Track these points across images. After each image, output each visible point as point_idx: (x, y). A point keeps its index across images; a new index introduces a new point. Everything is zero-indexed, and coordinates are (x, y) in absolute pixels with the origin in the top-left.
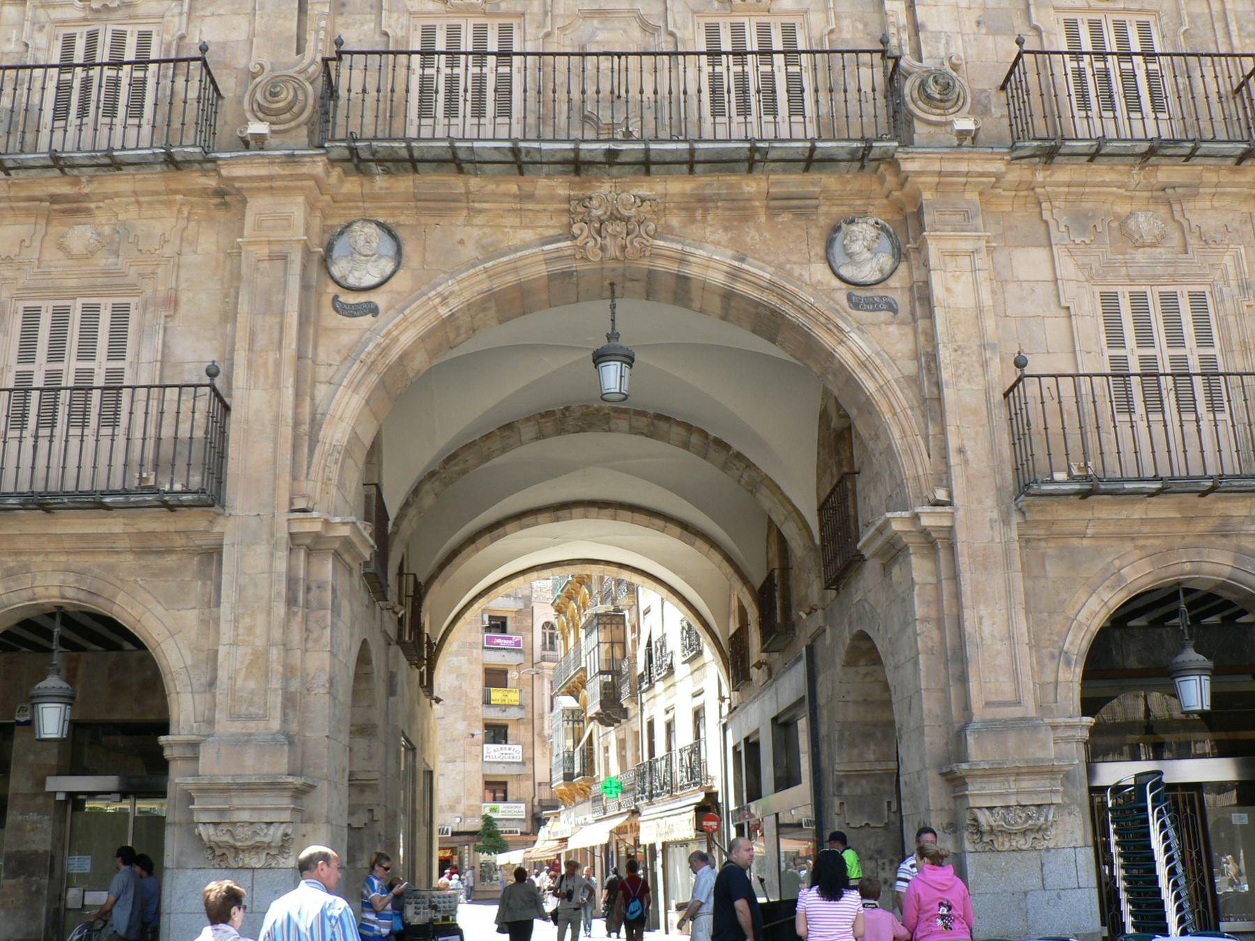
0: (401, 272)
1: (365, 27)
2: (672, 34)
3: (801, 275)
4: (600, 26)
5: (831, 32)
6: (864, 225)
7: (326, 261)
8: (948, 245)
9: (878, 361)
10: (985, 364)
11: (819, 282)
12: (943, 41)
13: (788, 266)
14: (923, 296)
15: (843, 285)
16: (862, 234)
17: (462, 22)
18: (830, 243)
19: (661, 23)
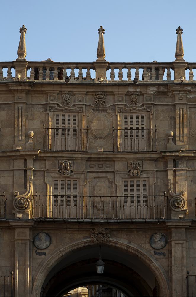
0: (51, 245)
1: (41, 181)
2: (115, 184)
3: (143, 246)
4: (98, 181)
5: (155, 183)
6: (159, 235)
7: (33, 242)
8: (177, 242)
9: (159, 268)
10: (182, 270)
11: (148, 248)
12: (182, 187)
13: (141, 244)
14: (170, 252)
15: (153, 249)
16: (158, 237)
17: (64, 180)
18: (151, 239)
19: (113, 181)
